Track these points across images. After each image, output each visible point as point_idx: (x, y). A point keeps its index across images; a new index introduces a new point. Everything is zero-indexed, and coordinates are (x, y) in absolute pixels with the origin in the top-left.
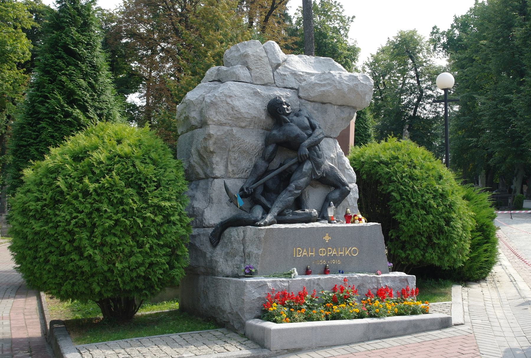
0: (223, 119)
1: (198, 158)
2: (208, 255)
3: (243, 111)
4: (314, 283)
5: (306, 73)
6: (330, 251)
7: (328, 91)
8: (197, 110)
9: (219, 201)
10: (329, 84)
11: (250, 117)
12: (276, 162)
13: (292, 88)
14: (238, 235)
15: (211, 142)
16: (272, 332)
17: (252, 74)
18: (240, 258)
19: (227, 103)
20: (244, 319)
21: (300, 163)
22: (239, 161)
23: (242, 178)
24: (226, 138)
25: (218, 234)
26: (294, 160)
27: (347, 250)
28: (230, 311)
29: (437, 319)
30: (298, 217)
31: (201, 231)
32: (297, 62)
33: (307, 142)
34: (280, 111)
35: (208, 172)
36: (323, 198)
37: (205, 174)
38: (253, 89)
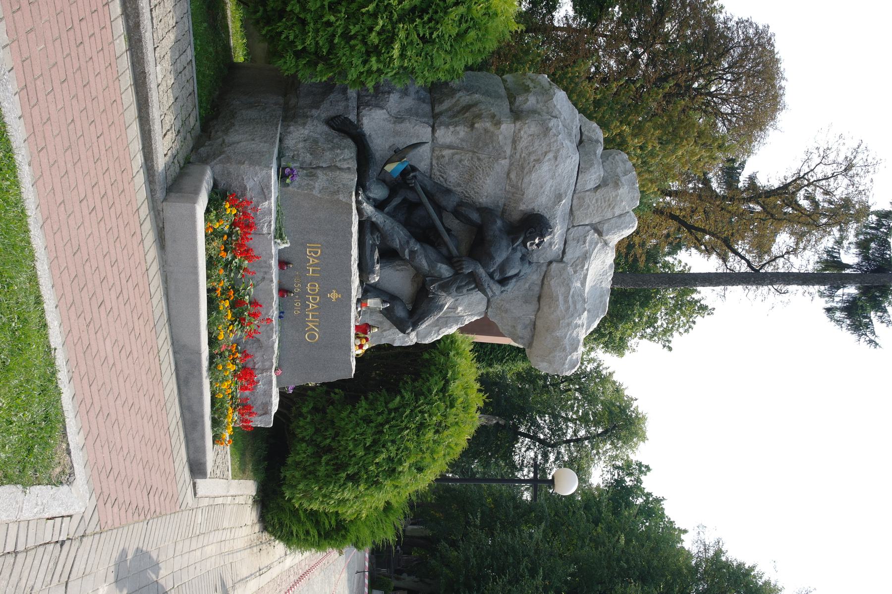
0: (522, 145)
1: (464, 104)
2: (315, 112)
3: (534, 176)
4: (266, 273)
5: (586, 275)
6: (314, 299)
7: (558, 306)
8: (539, 106)
9: (397, 133)
10: (568, 308)
11: (523, 186)
12: (454, 223)
13: (564, 252)
14: (344, 160)
15: (488, 125)
16: (188, 205)
17: (588, 193)
18: (308, 162)
19: (546, 153)
20: (213, 163)
21: (449, 260)
22: (457, 167)
23: (431, 169)
24: (494, 148)
25: (348, 129)
26: (454, 251)
28: (226, 141)
29: (205, 456)
30: (368, 252)
31: (353, 103)
32: (604, 262)
33: (481, 271)
35: (444, 118)
36: (396, 293)
37: (441, 113)
38: (566, 193)
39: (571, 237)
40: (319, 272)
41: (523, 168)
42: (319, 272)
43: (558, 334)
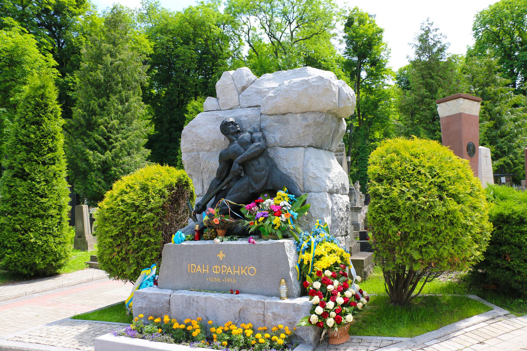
3: (204, 136)
4: (193, 300)
17: (220, 102)
27: (243, 269)
39: (247, 105)
40: (205, 265)
42: (205, 265)
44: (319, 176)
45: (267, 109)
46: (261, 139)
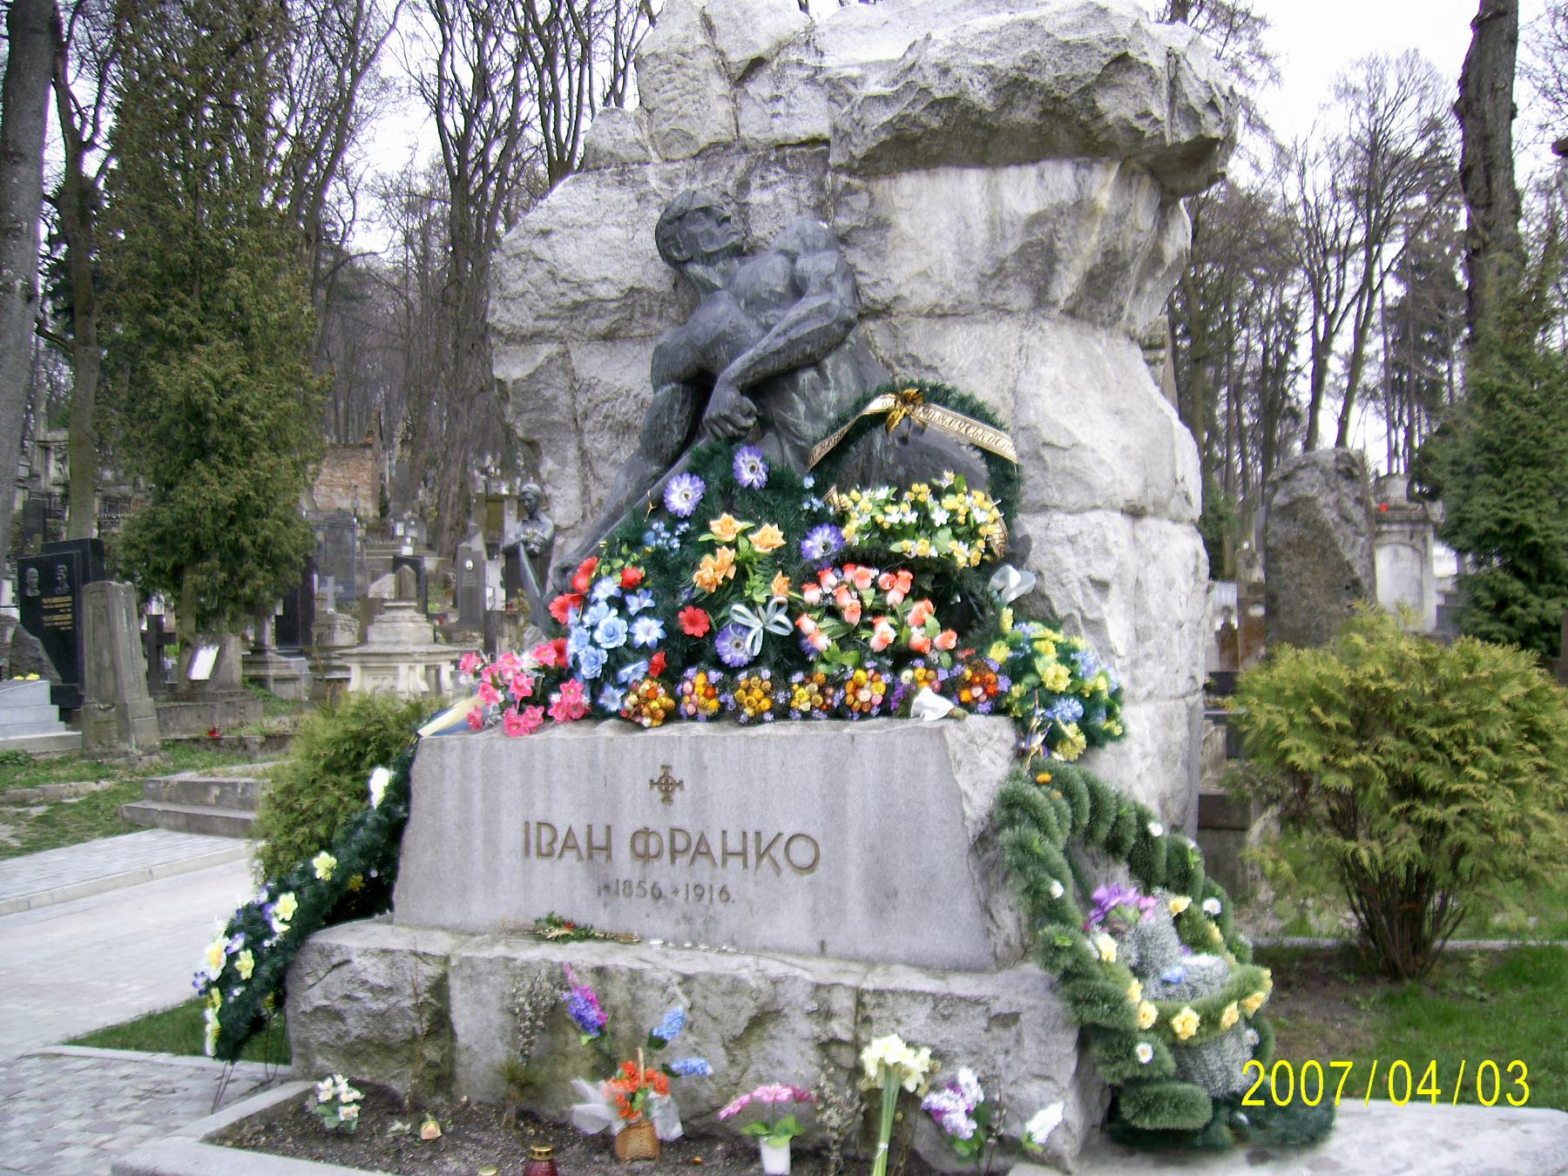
7: (903, 118)
11: (615, 294)
33: (737, 365)
34: (679, 250)
41: (577, 306)
43: (980, 95)
44: (1084, 440)
45: (858, 153)
46: (835, 281)
